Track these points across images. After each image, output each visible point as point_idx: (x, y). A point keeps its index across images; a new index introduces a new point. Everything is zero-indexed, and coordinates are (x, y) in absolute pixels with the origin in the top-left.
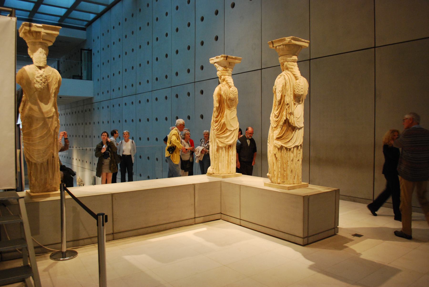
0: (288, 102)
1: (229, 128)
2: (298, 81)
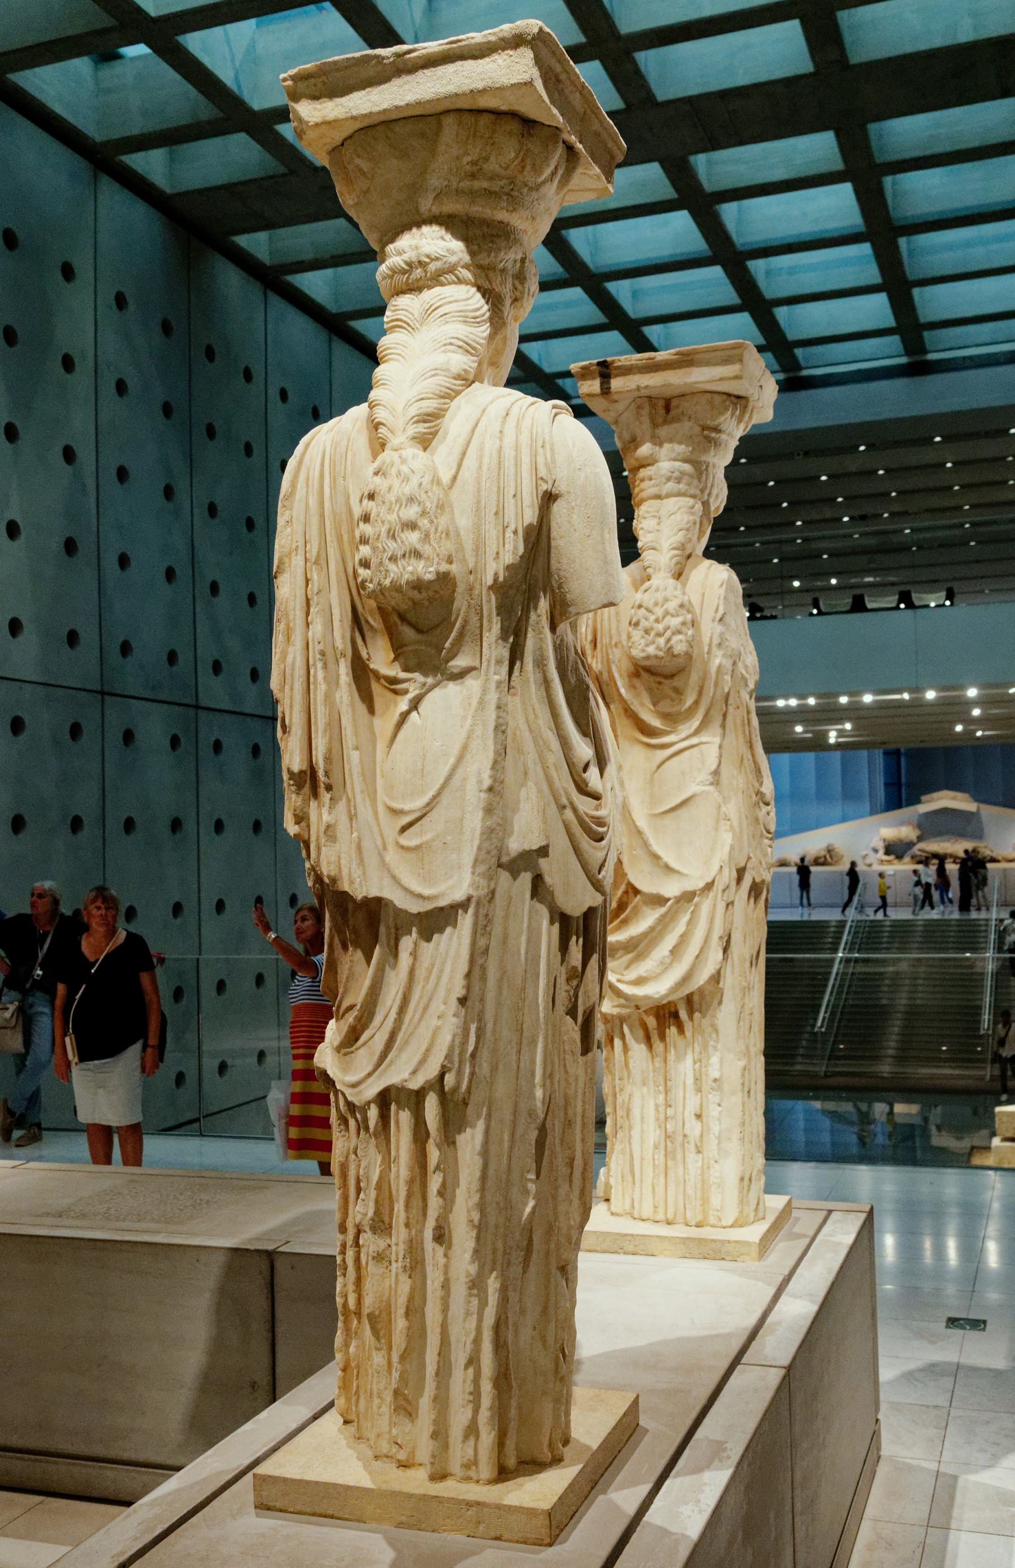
1: (645, 881)
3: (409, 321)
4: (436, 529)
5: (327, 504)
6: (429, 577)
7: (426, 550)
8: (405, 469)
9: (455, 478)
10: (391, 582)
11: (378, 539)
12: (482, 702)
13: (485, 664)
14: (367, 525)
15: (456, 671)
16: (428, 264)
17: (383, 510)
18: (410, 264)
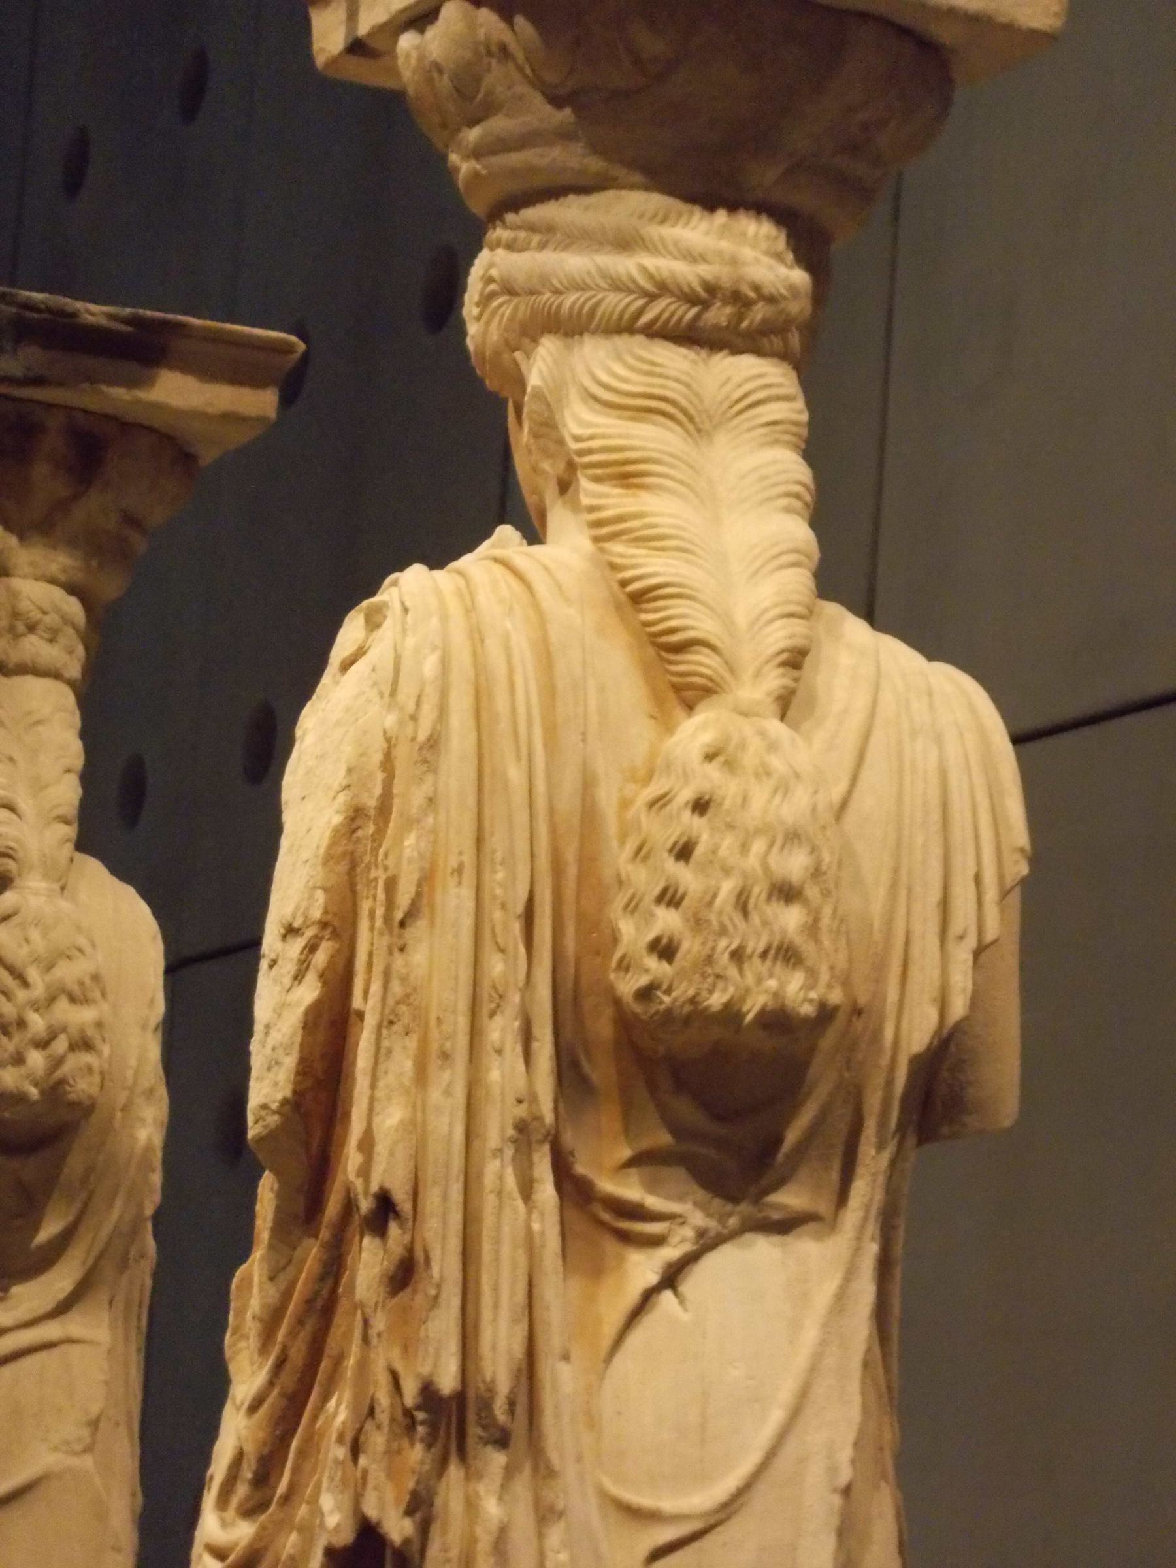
0: (390, 1172)
2: (696, 731)
3: (692, 411)
4: (835, 911)
5: (541, 787)
6: (807, 1010)
7: (807, 948)
8: (777, 763)
9: (844, 805)
10: (727, 1006)
11: (710, 904)
12: (841, 1297)
13: (852, 1215)
14: (681, 864)
15: (776, 1216)
16: (748, 304)
17: (728, 844)
18: (712, 289)
